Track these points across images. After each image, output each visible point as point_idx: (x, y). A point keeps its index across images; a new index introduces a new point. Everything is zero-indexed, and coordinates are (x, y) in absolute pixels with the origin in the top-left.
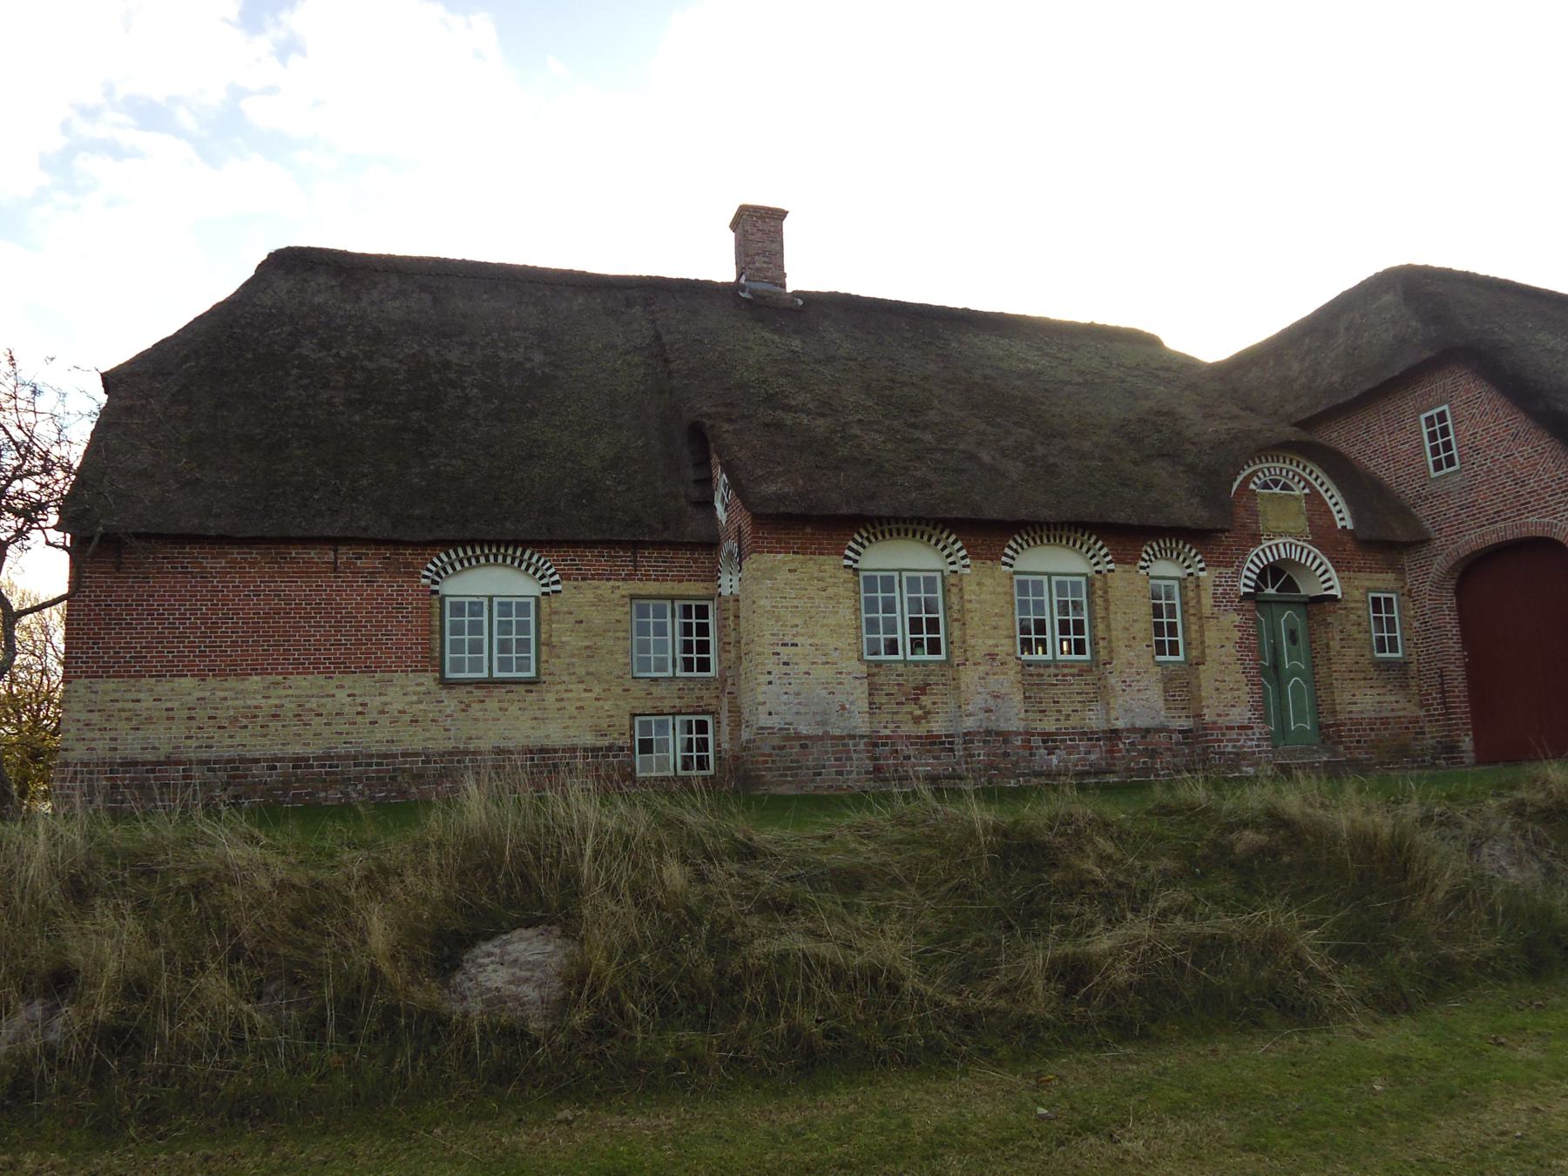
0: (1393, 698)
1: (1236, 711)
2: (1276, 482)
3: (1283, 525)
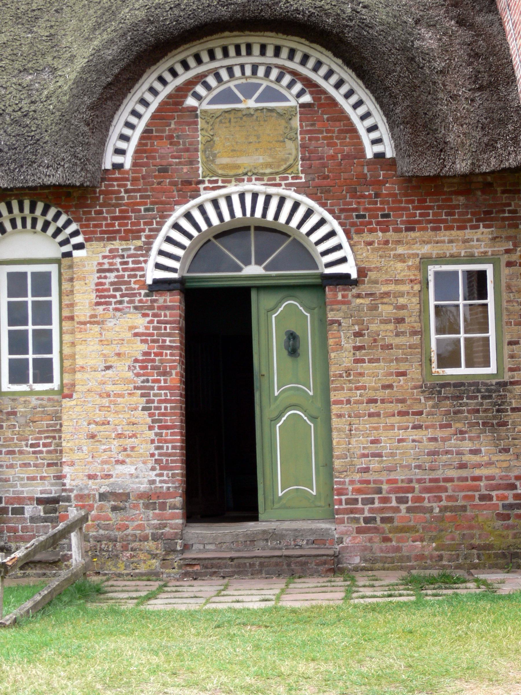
0: (467, 445)
2: (248, 91)
3: (246, 161)
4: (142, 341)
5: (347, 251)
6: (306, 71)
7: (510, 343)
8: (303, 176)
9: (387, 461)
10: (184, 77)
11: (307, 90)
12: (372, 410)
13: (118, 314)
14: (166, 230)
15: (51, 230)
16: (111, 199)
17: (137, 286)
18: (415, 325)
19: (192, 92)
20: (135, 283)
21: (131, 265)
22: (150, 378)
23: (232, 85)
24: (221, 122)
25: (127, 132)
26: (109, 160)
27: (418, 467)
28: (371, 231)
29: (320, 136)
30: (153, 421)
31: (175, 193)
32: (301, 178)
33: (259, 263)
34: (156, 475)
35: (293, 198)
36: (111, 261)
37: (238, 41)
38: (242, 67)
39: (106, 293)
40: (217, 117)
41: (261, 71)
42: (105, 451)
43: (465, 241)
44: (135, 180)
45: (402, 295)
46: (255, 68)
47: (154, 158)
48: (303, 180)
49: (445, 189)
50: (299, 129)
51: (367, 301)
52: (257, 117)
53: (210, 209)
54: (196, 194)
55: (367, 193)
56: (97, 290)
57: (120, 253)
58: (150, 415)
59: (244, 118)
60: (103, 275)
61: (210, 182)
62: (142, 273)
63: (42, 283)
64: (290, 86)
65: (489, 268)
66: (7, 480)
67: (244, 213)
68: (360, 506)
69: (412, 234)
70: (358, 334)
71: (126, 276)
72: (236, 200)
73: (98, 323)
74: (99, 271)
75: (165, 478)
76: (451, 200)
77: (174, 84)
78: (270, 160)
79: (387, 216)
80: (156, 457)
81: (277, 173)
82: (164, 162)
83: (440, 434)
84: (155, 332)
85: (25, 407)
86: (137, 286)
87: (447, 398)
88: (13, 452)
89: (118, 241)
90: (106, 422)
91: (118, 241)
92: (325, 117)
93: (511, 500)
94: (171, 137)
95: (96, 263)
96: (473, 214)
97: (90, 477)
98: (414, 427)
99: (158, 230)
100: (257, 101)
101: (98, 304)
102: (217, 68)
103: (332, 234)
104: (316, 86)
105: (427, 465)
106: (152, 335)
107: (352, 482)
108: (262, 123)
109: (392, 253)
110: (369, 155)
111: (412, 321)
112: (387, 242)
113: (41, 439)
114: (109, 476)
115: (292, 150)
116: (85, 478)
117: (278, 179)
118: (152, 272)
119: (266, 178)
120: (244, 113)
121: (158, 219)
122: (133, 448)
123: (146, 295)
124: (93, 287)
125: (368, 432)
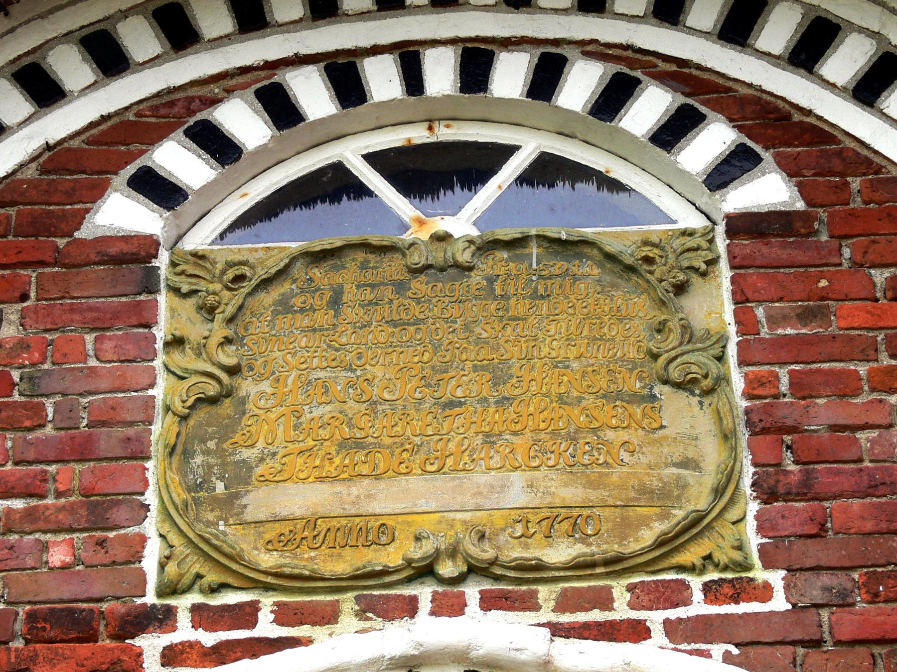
3: (423, 504)
8: (776, 578)
11: (767, 156)
19: (131, 170)
24: (284, 307)
29: (862, 369)
32: (765, 592)
40: (266, 283)
41: (510, 76)
46: (476, 65)
48: (779, 603)
50: (734, 340)
52: (491, 280)
59: (419, 285)
61: (203, 617)
64: (673, 131)
78: (571, 493)
81: (616, 565)
92: (880, 276)
102: (272, 66)
108: (518, 307)
115: (697, 443)
119: (546, 593)
120: (417, 258)
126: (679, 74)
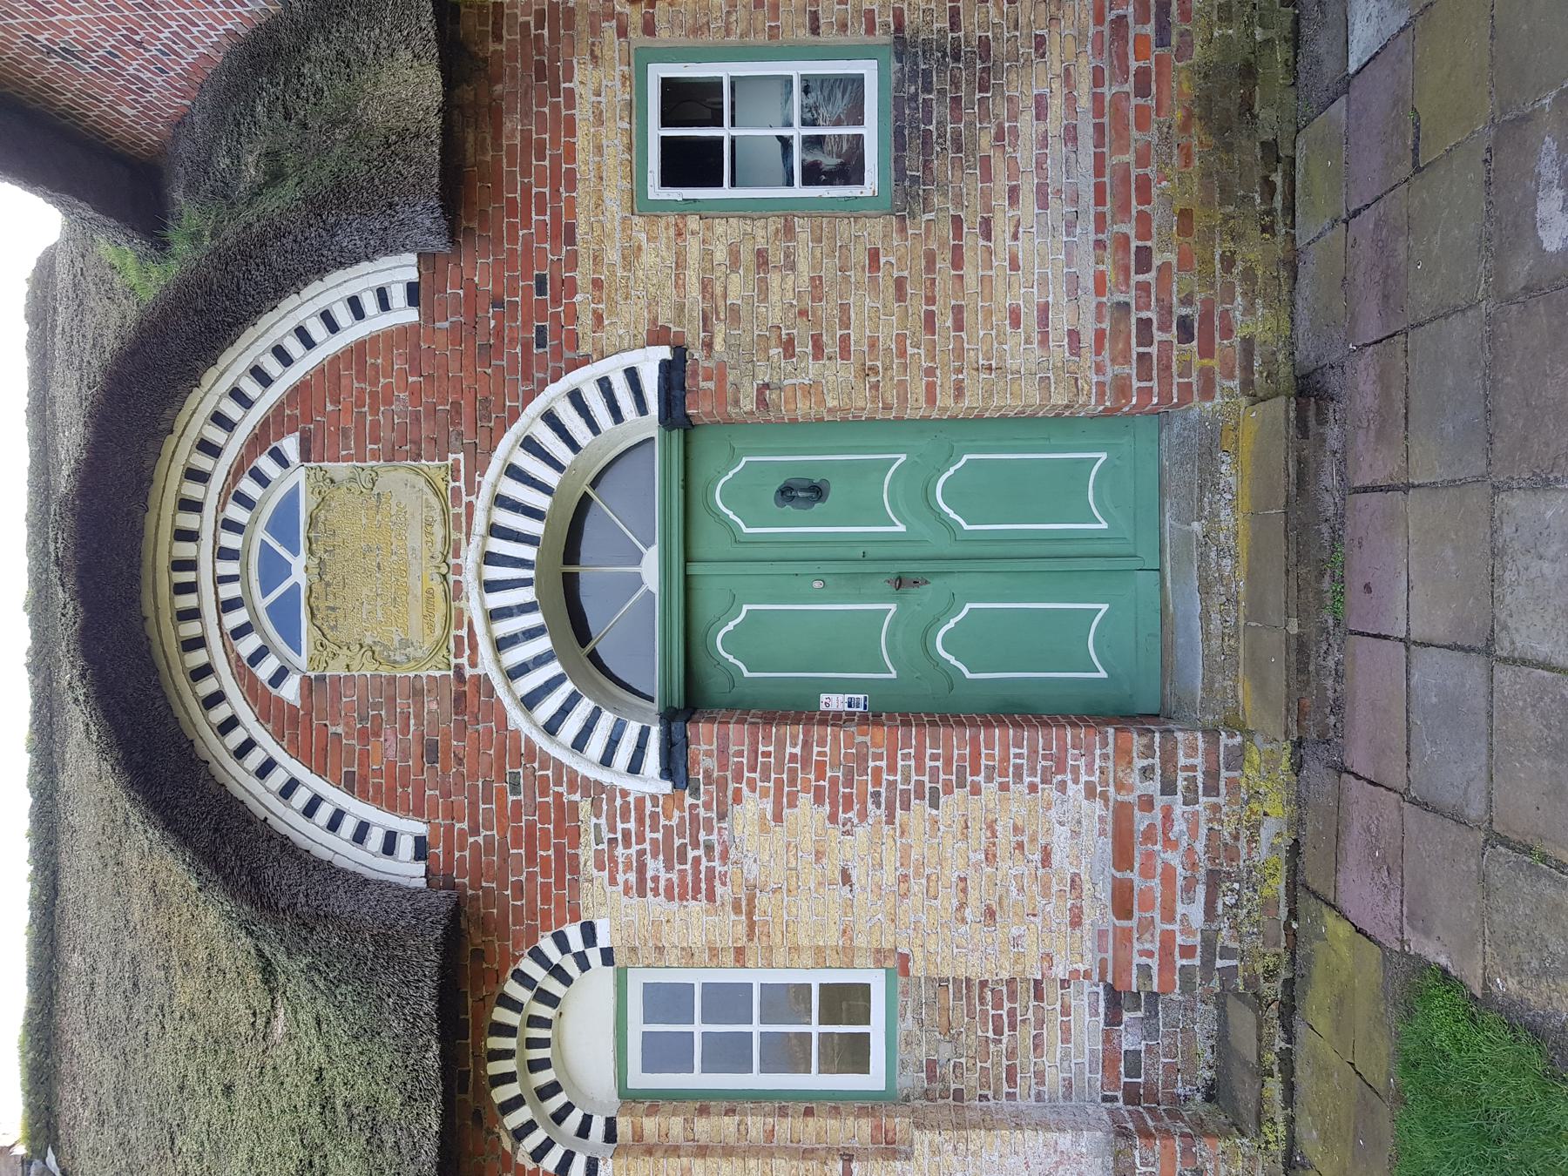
0: (1027, 124)
1: (1060, 839)
2: (274, 570)
4: (792, 805)
5: (612, 368)
6: (233, 446)
7: (815, 30)
9: (1056, 295)
10: (237, 703)
12: (949, 323)
13: (733, 854)
14: (558, 749)
15: (554, 987)
16: (490, 864)
17: (676, 813)
18: (772, 228)
19: (270, 688)
20: (669, 818)
21: (632, 825)
22: (870, 789)
23: (262, 603)
25: (348, 827)
26: (407, 870)
27: (1070, 226)
28: (573, 316)
29: (369, 418)
30: (962, 785)
31: (480, 727)
32: (457, 461)
33: (638, 558)
34: (1076, 781)
35: (498, 479)
36: (621, 867)
37: (164, 589)
38: (221, 580)
39: (689, 879)
41: (231, 540)
42: (1021, 889)
43: (599, 120)
44: (451, 813)
45: (708, 255)
47: (406, 771)
48: (461, 456)
49: (489, 158)
51: (720, 331)
53: (514, 656)
54: (483, 683)
55: (493, 323)
56: (682, 897)
57: (605, 846)
58: (949, 792)
59: (327, 578)
60: (650, 884)
62: (648, 803)
63: (667, 1001)
64: (262, 479)
65: (657, 72)
66: (1069, 1085)
67: (526, 583)
68: (1154, 350)
69: (581, 230)
70: (789, 346)
71: (655, 835)
72: (498, 600)
73: (751, 900)
74: (642, 893)
75: (1082, 762)
76: (512, 149)
77: (251, 725)
79: (541, 281)
80: (1038, 780)
82: (415, 749)
83: (1001, 183)
84: (773, 776)
85: (919, 1045)
86: (676, 813)
87: (927, 165)
88: (1011, 1072)
89: (580, 852)
90: (961, 885)
91: (580, 852)
92: (329, 407)
93: (1150, 29)
94: (364, 736)
95: (625, 899)
96: (541, 104)
97: (1076, 922)
98: (988, 237)
99: (559, 765)
100: (296, 553)
101: (711, 897)
103: (576, 398)
104: (265, 424)
105: (1066, 209)
106: (779, 784)
107: (1099, 369)
108: (338, 540)
109: (620, 273)
110: (412, 316)
111: (762, 233)
112: (597, 284)
113: (984, 1013)
114: (1075, 883)
116: (1078, 932)
117: (457, 510)
118: (646, 781)
120: (316, 579)
121: (536, 765)
122: (1017, 830)
123: (695, 793)
124: (675, 904)
125: (994, 333)
126: (236, 473)
